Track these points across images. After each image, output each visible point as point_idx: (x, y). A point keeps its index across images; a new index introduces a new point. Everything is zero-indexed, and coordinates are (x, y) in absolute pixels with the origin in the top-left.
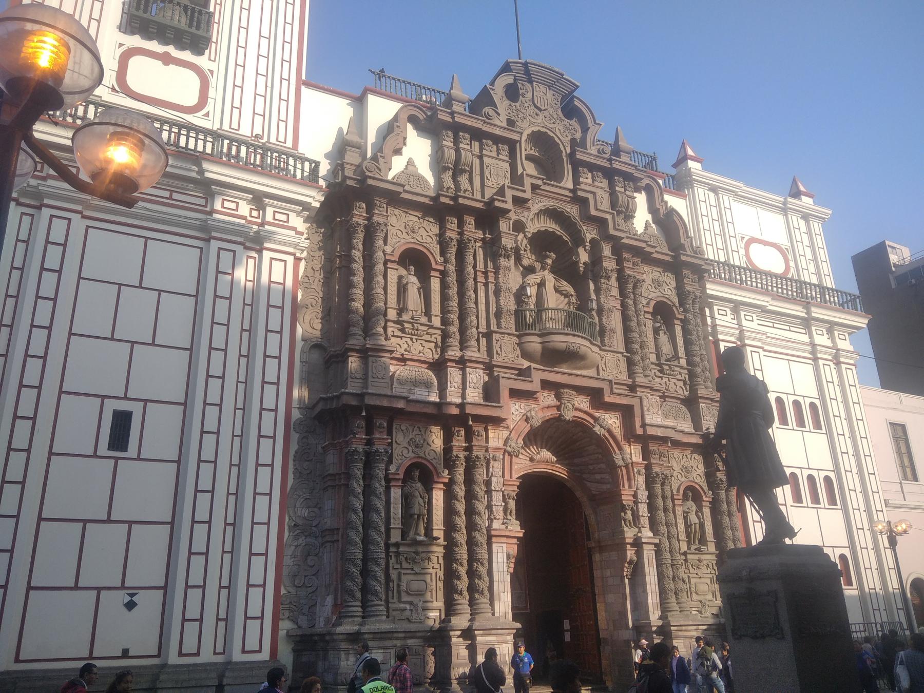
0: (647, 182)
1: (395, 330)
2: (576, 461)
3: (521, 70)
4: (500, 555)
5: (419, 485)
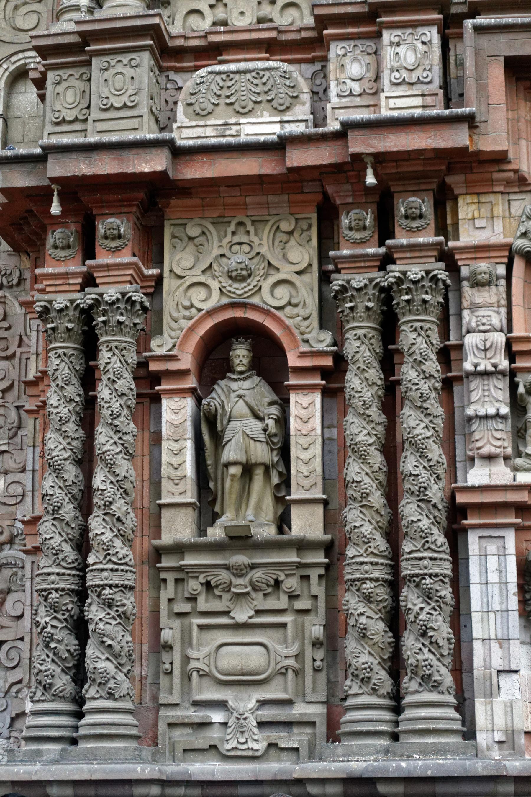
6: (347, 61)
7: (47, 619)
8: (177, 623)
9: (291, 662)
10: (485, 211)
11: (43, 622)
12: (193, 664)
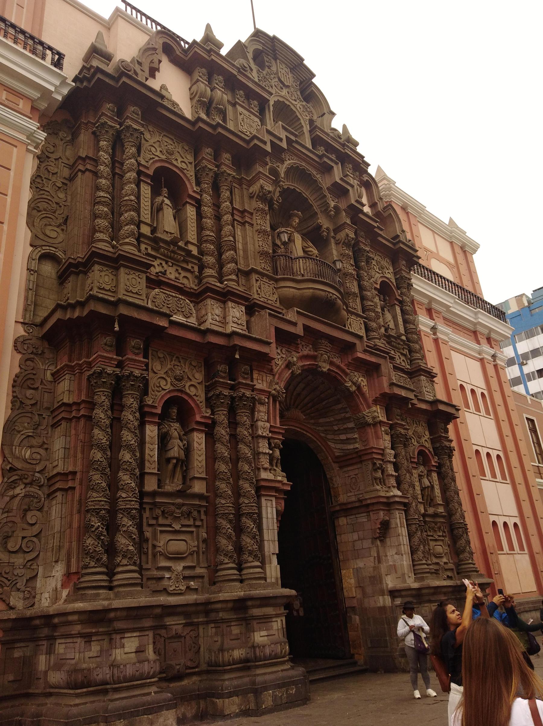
0: (367, 178)
2: (321, 421)
4: (269, 509)
5: (177, 425)
7: (99, 524)
8: (150, 529)
9: (196, 549)
11: (97, 525)
12: (158, 549)
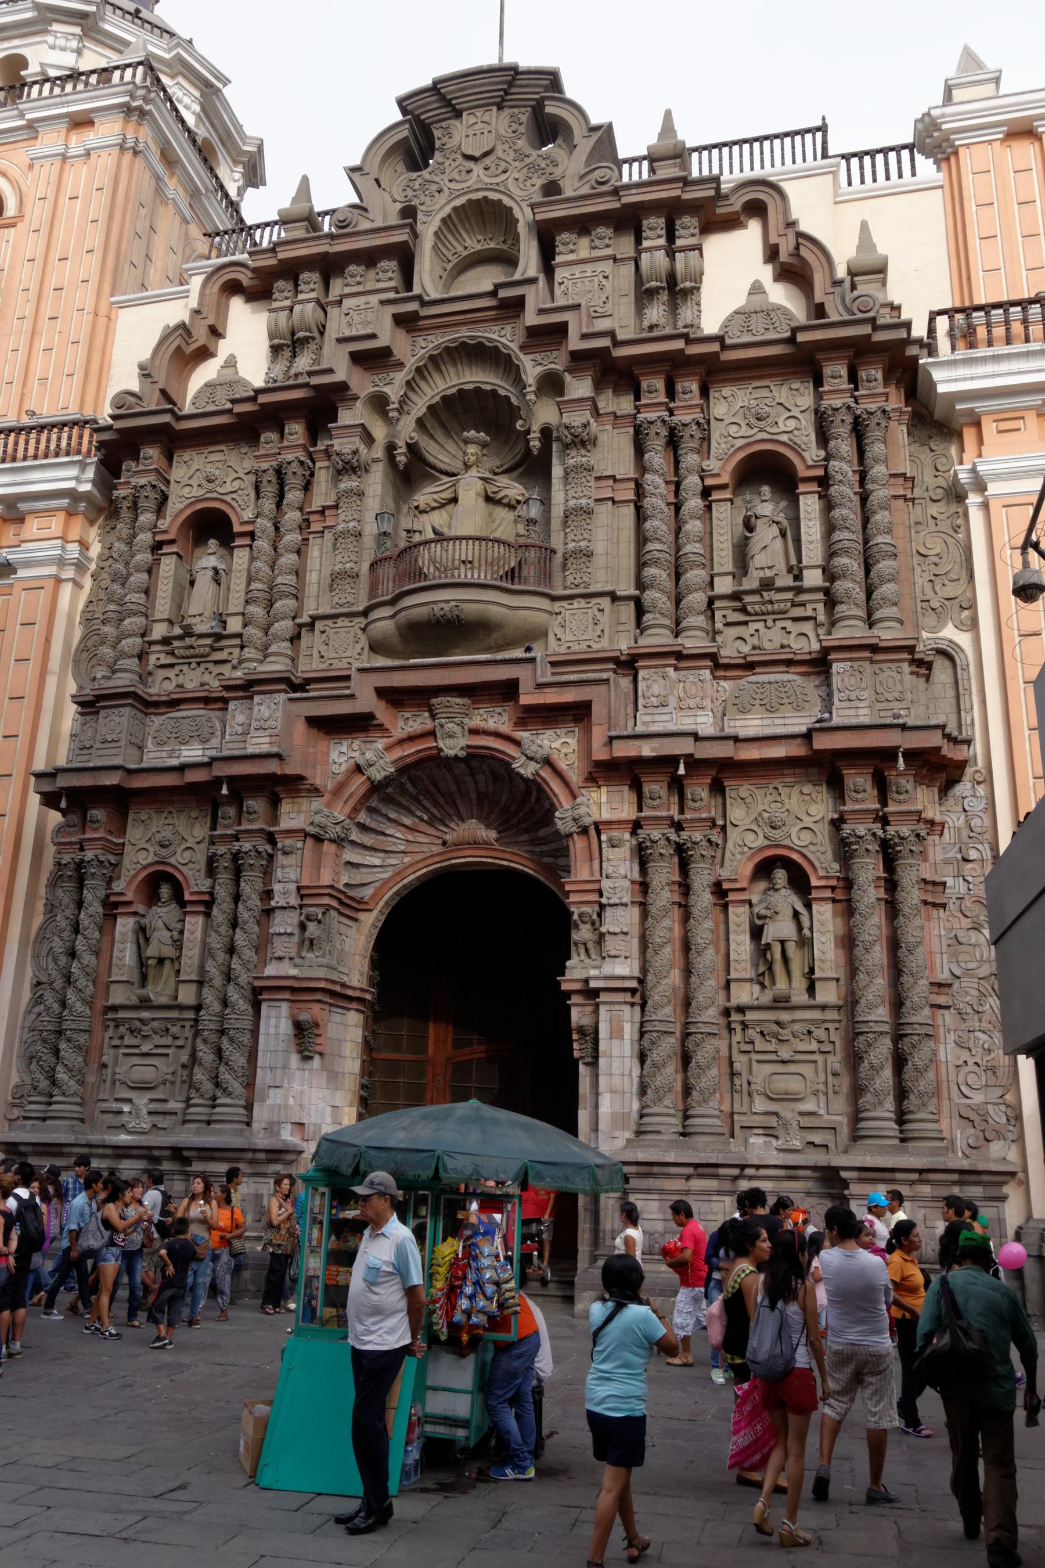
1: (162, 656)
3: (429, 103)
6: (237, 713)
8: (112, 1051)
9: (168, 1077)
10: (296, 808)
